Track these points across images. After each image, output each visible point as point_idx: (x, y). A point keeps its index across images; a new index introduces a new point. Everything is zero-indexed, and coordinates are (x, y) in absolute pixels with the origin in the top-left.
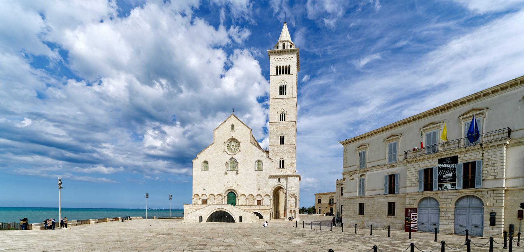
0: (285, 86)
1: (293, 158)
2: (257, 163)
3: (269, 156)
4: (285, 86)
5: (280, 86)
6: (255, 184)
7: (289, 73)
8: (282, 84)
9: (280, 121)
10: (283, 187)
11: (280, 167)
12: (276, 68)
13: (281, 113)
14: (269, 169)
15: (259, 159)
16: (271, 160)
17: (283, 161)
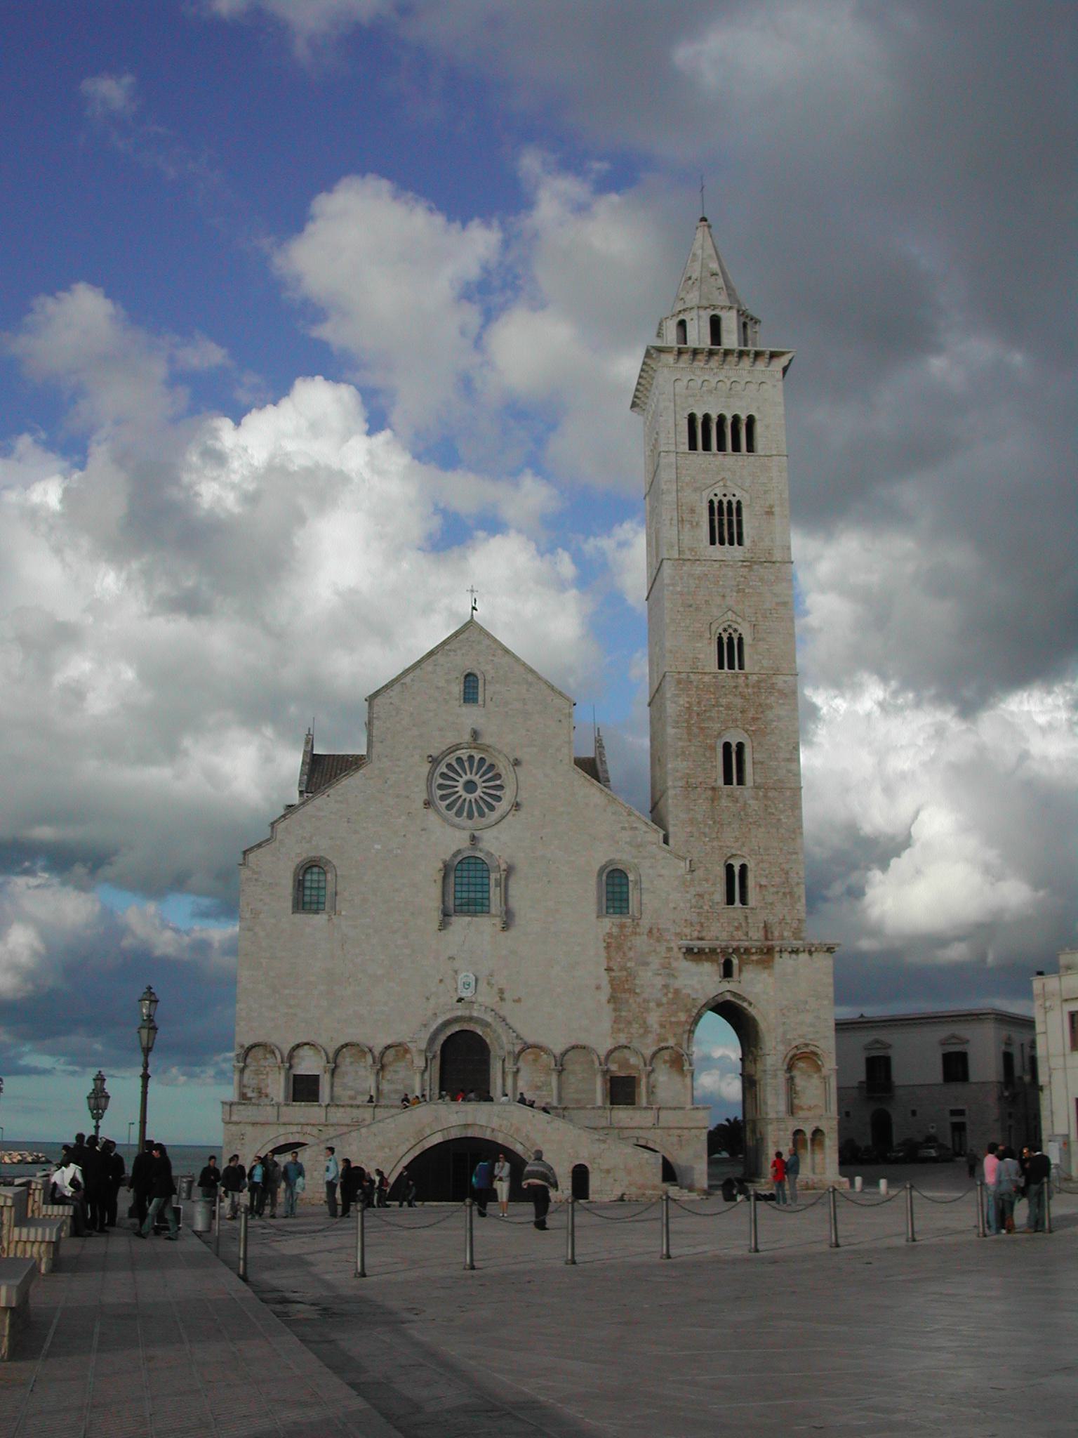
0: (734, 506)
1: (794, 856)
2: (604, 878)
3: (671, 841)
4: (734, 506)
5: (711, 502)
6: (598, 988)
7: (750, 448)
8: (720, 497)
9: (721, 667)
10: (750, 1004)
11: (730, 901)
12: (687, 420)
13: (720, 631)
14: (675, 908)
15: (617, 856)
16: (682, 864)
17: (744, 868)
